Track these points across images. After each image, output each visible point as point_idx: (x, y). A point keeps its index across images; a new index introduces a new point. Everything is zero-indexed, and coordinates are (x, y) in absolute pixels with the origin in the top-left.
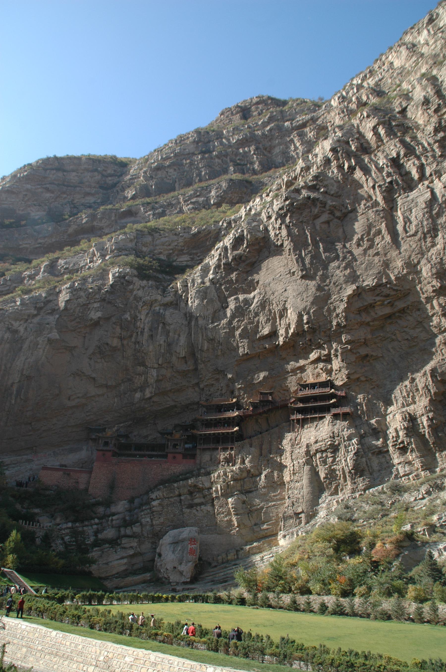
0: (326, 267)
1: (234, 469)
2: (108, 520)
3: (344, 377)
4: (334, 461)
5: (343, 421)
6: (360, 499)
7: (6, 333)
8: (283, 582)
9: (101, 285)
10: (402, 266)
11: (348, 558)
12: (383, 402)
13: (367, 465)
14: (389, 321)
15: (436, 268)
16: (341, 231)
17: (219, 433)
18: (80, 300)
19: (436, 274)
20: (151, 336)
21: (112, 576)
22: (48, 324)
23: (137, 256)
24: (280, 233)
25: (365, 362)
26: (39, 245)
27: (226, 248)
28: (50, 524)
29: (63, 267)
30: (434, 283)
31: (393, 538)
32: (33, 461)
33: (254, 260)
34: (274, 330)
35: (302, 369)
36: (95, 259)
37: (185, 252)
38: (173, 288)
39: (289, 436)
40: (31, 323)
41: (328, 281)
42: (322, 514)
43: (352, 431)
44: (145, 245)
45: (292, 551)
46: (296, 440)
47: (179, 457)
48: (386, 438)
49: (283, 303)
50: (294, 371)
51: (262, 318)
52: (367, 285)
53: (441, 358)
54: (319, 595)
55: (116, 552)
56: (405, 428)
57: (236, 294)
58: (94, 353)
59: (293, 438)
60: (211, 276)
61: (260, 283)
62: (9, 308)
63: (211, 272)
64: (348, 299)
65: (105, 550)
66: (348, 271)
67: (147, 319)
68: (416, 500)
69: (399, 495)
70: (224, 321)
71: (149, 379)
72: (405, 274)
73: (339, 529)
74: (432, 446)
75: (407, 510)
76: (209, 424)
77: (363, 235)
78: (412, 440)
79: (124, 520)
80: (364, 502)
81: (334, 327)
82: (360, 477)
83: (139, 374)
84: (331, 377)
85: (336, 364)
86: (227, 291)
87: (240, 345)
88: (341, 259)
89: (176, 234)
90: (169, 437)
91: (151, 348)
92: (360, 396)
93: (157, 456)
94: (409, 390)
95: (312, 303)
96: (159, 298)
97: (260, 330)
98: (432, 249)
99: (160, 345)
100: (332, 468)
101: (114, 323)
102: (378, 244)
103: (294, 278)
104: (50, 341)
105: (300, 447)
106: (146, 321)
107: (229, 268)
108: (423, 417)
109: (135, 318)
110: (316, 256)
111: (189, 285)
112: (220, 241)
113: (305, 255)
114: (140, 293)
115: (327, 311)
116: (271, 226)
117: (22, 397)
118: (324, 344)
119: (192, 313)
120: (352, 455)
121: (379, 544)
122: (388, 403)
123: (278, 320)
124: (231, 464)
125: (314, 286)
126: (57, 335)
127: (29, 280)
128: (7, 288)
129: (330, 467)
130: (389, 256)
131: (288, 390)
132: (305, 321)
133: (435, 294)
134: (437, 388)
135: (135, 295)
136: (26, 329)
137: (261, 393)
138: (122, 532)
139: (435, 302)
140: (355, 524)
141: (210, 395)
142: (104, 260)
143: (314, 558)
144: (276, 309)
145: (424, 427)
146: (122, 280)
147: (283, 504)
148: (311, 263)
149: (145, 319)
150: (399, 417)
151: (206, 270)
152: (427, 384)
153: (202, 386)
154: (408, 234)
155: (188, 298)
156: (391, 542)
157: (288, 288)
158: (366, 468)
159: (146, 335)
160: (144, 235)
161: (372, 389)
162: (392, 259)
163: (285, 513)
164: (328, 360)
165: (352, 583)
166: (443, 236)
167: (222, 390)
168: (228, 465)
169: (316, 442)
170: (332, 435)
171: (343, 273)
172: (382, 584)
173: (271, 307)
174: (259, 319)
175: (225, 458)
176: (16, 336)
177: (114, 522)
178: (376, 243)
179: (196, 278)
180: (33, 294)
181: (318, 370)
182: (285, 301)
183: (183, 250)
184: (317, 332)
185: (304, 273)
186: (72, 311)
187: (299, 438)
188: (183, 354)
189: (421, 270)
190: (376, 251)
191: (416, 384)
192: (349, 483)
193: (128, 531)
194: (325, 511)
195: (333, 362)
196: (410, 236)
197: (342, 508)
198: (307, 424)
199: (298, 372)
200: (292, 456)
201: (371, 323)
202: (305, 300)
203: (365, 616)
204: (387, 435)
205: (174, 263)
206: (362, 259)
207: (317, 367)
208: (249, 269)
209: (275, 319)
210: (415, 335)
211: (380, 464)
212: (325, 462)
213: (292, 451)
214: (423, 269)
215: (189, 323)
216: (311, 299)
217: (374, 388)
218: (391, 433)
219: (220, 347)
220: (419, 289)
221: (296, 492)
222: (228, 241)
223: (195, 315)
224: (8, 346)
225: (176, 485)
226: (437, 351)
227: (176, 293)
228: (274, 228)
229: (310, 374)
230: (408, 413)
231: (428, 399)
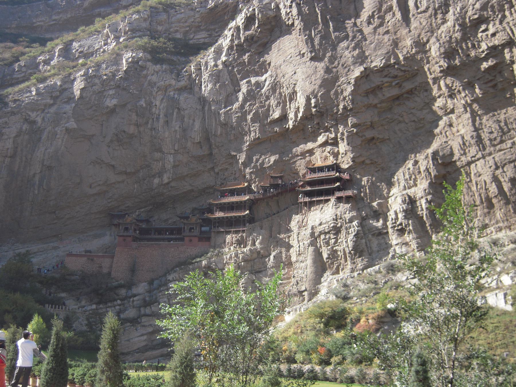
0: (334, 48)
1: (245, 250)
2: (129, 302)
3: (349, 160)
4: (336, 242)
5: (345, 204)
6: (358, 278)
7: (24, 124)
8: (273, 353)
9: (115, 71)
10: (411, 45)
11: (335, 332)
12: (387, 185)
13: (366, 245)
14: (397, 103)
15: (445, 47)
16: (352, 7)
17: (231, 217)
18: (95, 88)
19: (443, 53)
20: (167, 122)
21: (133, 351)
22: (65, 113)
23: (153, 37)
24: (291, 12)
25: (371, 144)
26: (54, 22)
27: (238, 28)
28: (77, 307)
29: (77, 50)
30: (442, 63)
31: (376, 314)
32: (59, 248)
33: (266, 41)
34: (284, 114)
35: (311, 152)
36: (109, 41)
37: (202, 28)
38: (186, 71)
39: (296, 219)
40: (48, 113)
41: (336, 63)
42: (323, 290)
43: (354, 213)
44: (160, 23)
45: (289, 326)
46: (303, 223)
47: (195, 240)
48: (386, 220)
49: (293, 86)
50: (303, 154)
51: (273, 102)
52: (375, 67)
53: (445, 140)
54: (303, 363)
55: (136, 330)
56: (404, 211)
57: (249, 77)
58: (112, 141)
59: (301, 220)
60: (223, 58)
61: (272, 64)
62: (26, 98)
63: (224, 54)
64: (355, 81)
65: (127, 328)
66: (357, 51)
67: (162, 105)
68: (407, 279)
69: (393, 274)
70: (236, 105)
71: (166, 165)
72: (414, 54)
73: (329, 307)
74: (429, 228)
75: (397, 288)
76: (223, 208)
77: (374, 12)
78: (410, 222)
79: (144, 300)
80: (360, 280)
81: (341, 110)
82: (359, 257)
83: (157, 160)
84: (337, 160)
85: (343, 147)
86: (239, 74)
87: (252, 129)
88: (350, 39)
89: (192, 10)
90: (185, 221)
91: (167, 134)
92: (365, 179)
93: (176, 239)
94: (411, 172)
95: (320, 86)
96: (173, 82)
97: (271, 112)
98: (442, 27)
99: (176, 131)
100: (334, 249)
101: (130, 110)
102: (388, 22)
103: (305, 59)
104: (68, 131)
105: (306, 229)
106: (162, 107)
107: (241, 49)
108: (422, 200)
109: (150, 104)
110: (325, 37)
111: (202, 68)
112: (233, 20)
113: (315, 35)
114: (154, 78)
115: (334, 94)
116: (282, 4)
117: (44, 187)
118: (331, 127)
119: (205, 97)
120: (352, 237)
121: (363, 320)
122: (390, 185)
123: (288, 103)
124: (242, 246)
125: (323, 68)
126: (75, 124)
127: (44, 66)
128: (23, 75)
129: (332, 248)
130: (398, 33)
131: (297, 173)
132: (313, 105)
133: (442, 74)
134: (437, 171)
135: (149, 81)
136: (43, 119)
137: (272, 177)
138: (143, 312)
139: (442, 83)
140: (350, 301)
141: (225, 179)
142: (118, 43)
143: (306, 332)
144: (286, 91)
145: (422, 210)
146: (136, 66)
147: (290, 282)
148: (320, 44)
149: (161, 105)
150: (399, 200)
151: (218, 53)
152: (428, 167)
153: (216, 170)
154: (419, 11)
155: (201, 82)
156: (373, 318)
157: (297, 71)
158: (366, 249)
159: (161, 121)
160: (158, 12)
161: (376, 172)
162: (402, 37)
163: (290, 291)
164: (335, 143)
165: (330, 354)
166: (454, 12)
167: (235, 174)
168: (240, 247)
169: (320, 224)
170: (335, 217)
171: (352, 53)
172: (354, 354)
173: (282, 90)
174: (270, 103)
175: (238, 240)
176: (34, 127)
177: (135, 303)
178: (386, 21)
179: (209, 61)
180: (49, 82)
181: (326, 153)
182: (295, 84)
183: (201, 26)
184: (325, 115)
185: (313, 54)
186: (88, 99)
187: (305, 221)
188: (197, 139)
189: (430, 49)
190: (386, 29)
191: (419, 167)
192: (349, 262)
193: (148, 311)
194: (326, 289)
195: (340, 145)
196: (421, 13)
197: (340, 288)
198: (314, 206)
199: (307, 155)
200: (298, 238)
201: (379, 106)
202: (313, 83)
203: (333, 380)
204: (387, 216)
205: (191, 42)
206: (372, 38)
207: (325, 151)
208: (262, 50)
209: (285, 102)
210: (422, 117)
211: (379, 245)
212: (327, 243)
213: (299, 233)
214: (432, 48)
215: (203, 108)
216: (319, 82)
217: (379, 170)
218: (391, 215)
219: (233, 132)
220: (426, 70)
221: (300, 271)
222: (240, 20)
223: (208, 99)
224: (27, 137)
225: (191, 267)
226: (441, 133)
227: (190, 77)
228: (285, 6)
229: (319, 157)
230: (408, 195)
231: (428, 182)
